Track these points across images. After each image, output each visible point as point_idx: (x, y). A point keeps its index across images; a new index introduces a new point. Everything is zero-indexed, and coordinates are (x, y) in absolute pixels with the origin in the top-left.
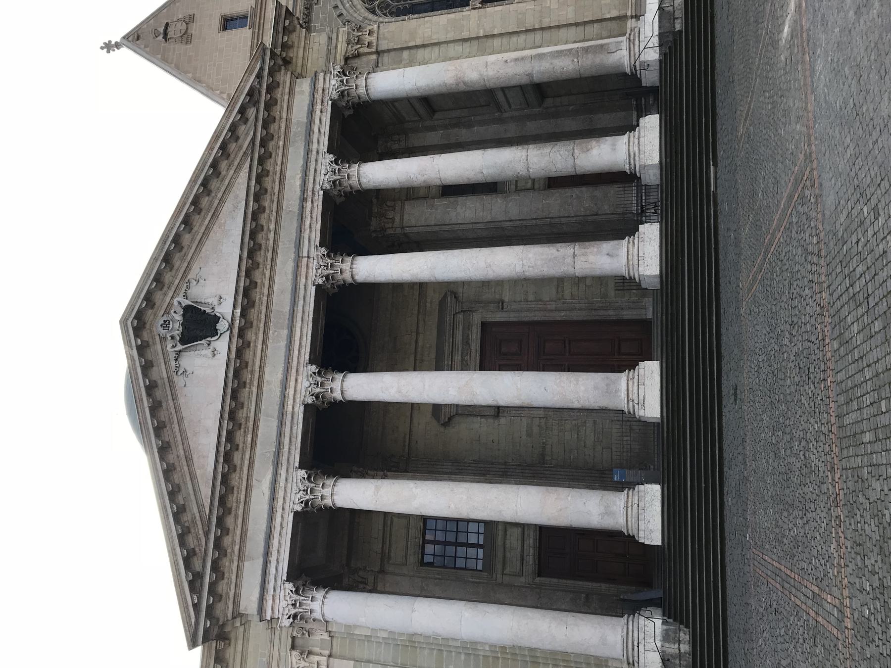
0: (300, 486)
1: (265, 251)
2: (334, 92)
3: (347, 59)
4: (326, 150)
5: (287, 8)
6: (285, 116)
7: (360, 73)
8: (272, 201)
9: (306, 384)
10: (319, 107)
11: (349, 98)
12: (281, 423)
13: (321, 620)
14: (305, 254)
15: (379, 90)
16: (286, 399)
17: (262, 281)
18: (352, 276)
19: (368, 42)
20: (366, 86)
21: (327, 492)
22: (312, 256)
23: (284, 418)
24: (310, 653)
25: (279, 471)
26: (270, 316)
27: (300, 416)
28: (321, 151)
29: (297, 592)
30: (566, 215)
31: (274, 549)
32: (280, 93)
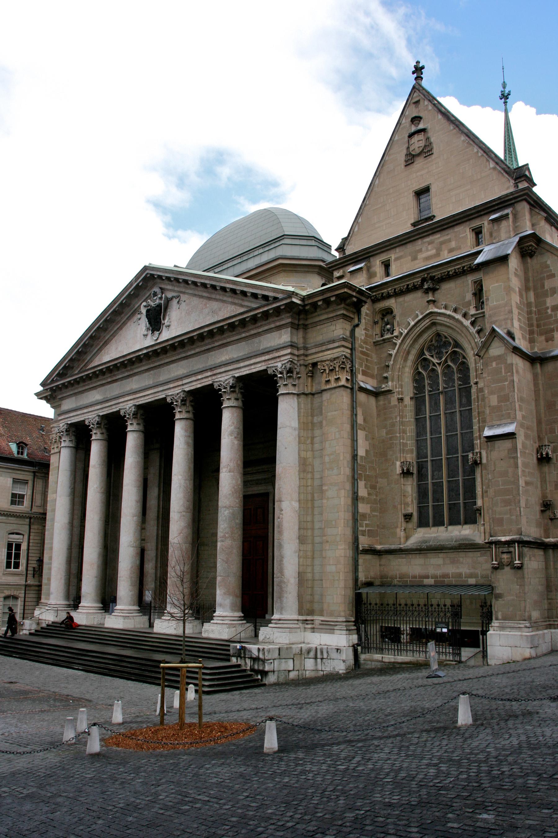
2: (274, 369)
6: (260, 330)
8: (209, 344)
10: (267, 357)
14: (185, 381)
28: (240, 370)
32: (273, 320)
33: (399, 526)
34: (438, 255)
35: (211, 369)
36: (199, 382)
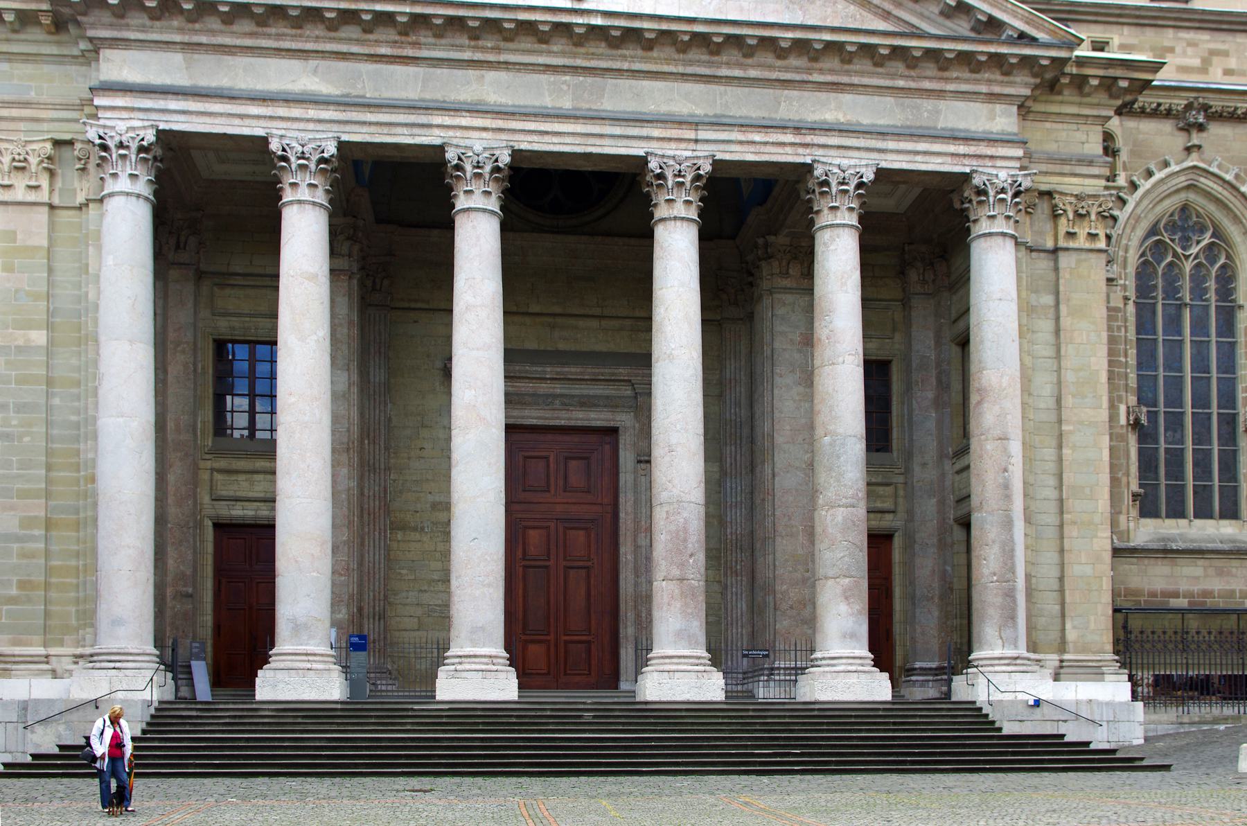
0: (310, 146)
1: (709, 62)
2: (985, 178)
3: (1049, 194)
4: (884, 165)
5: (1153, 81)
7: (1017, 222)
9: (478, 147)
10: (962, 149)
11: (974, 203)
12: (412, 108)
13: (103, 191)
14: (702, 135)
15: (984, 257)
16: (452, 113)
17: (655, 59)
18: (663, 220)
19: (1075, 234)
20: (990, 234)
21: (304, 194)
22: (699, 147)
23: (421, 111)
24: (52, 173)
25: (332, 107)
26: (595, 75)
27: (424, 138)
28: (883, 156)
29: (142, 149)
30: (777, 563)
31: (207, 105)
33: (1124, 510)
34: (1204, 70)
35: (797, 130)
36: (752, 148)
